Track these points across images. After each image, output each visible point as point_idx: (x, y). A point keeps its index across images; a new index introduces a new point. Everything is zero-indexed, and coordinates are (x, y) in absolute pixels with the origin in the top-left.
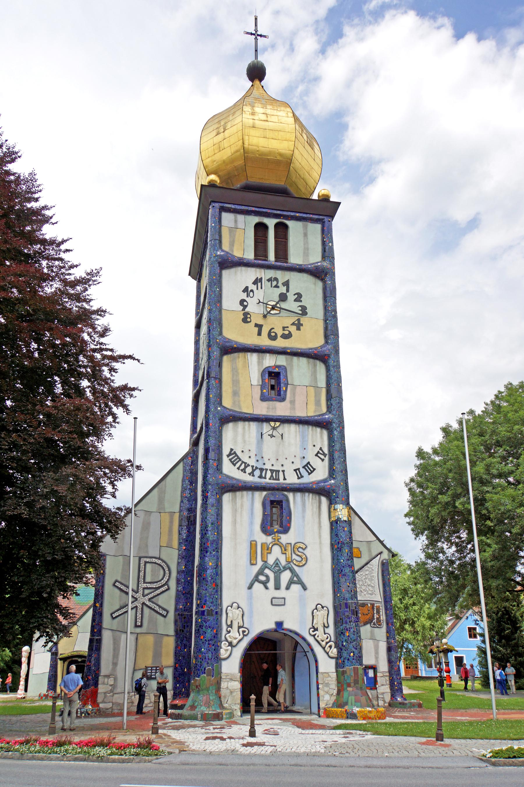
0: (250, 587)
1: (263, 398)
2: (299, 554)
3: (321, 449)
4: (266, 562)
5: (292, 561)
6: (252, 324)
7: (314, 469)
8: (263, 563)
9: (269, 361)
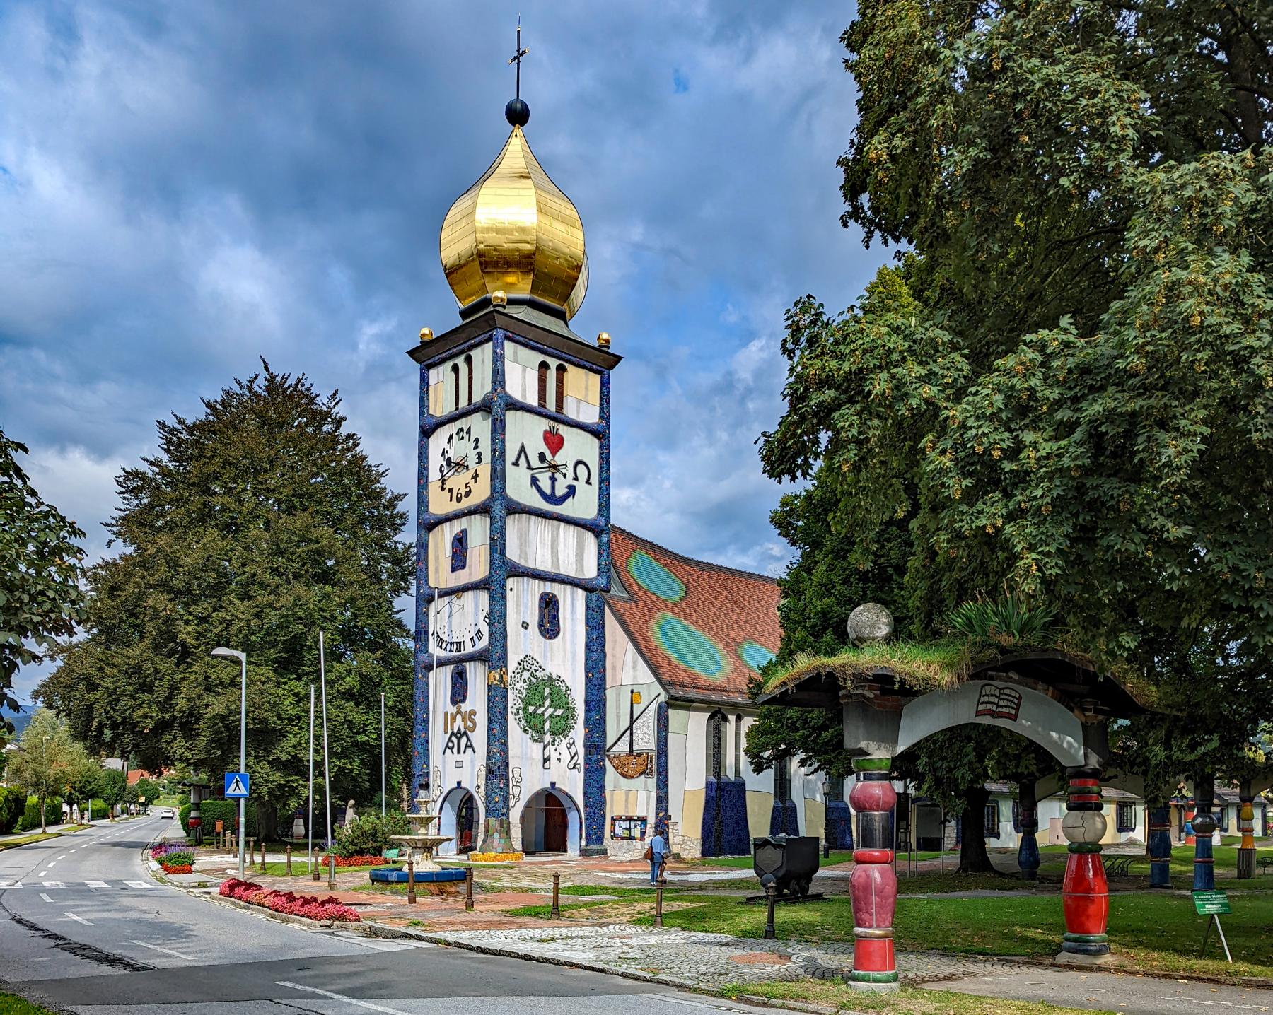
6: (447, 490)
9: (457, 526)
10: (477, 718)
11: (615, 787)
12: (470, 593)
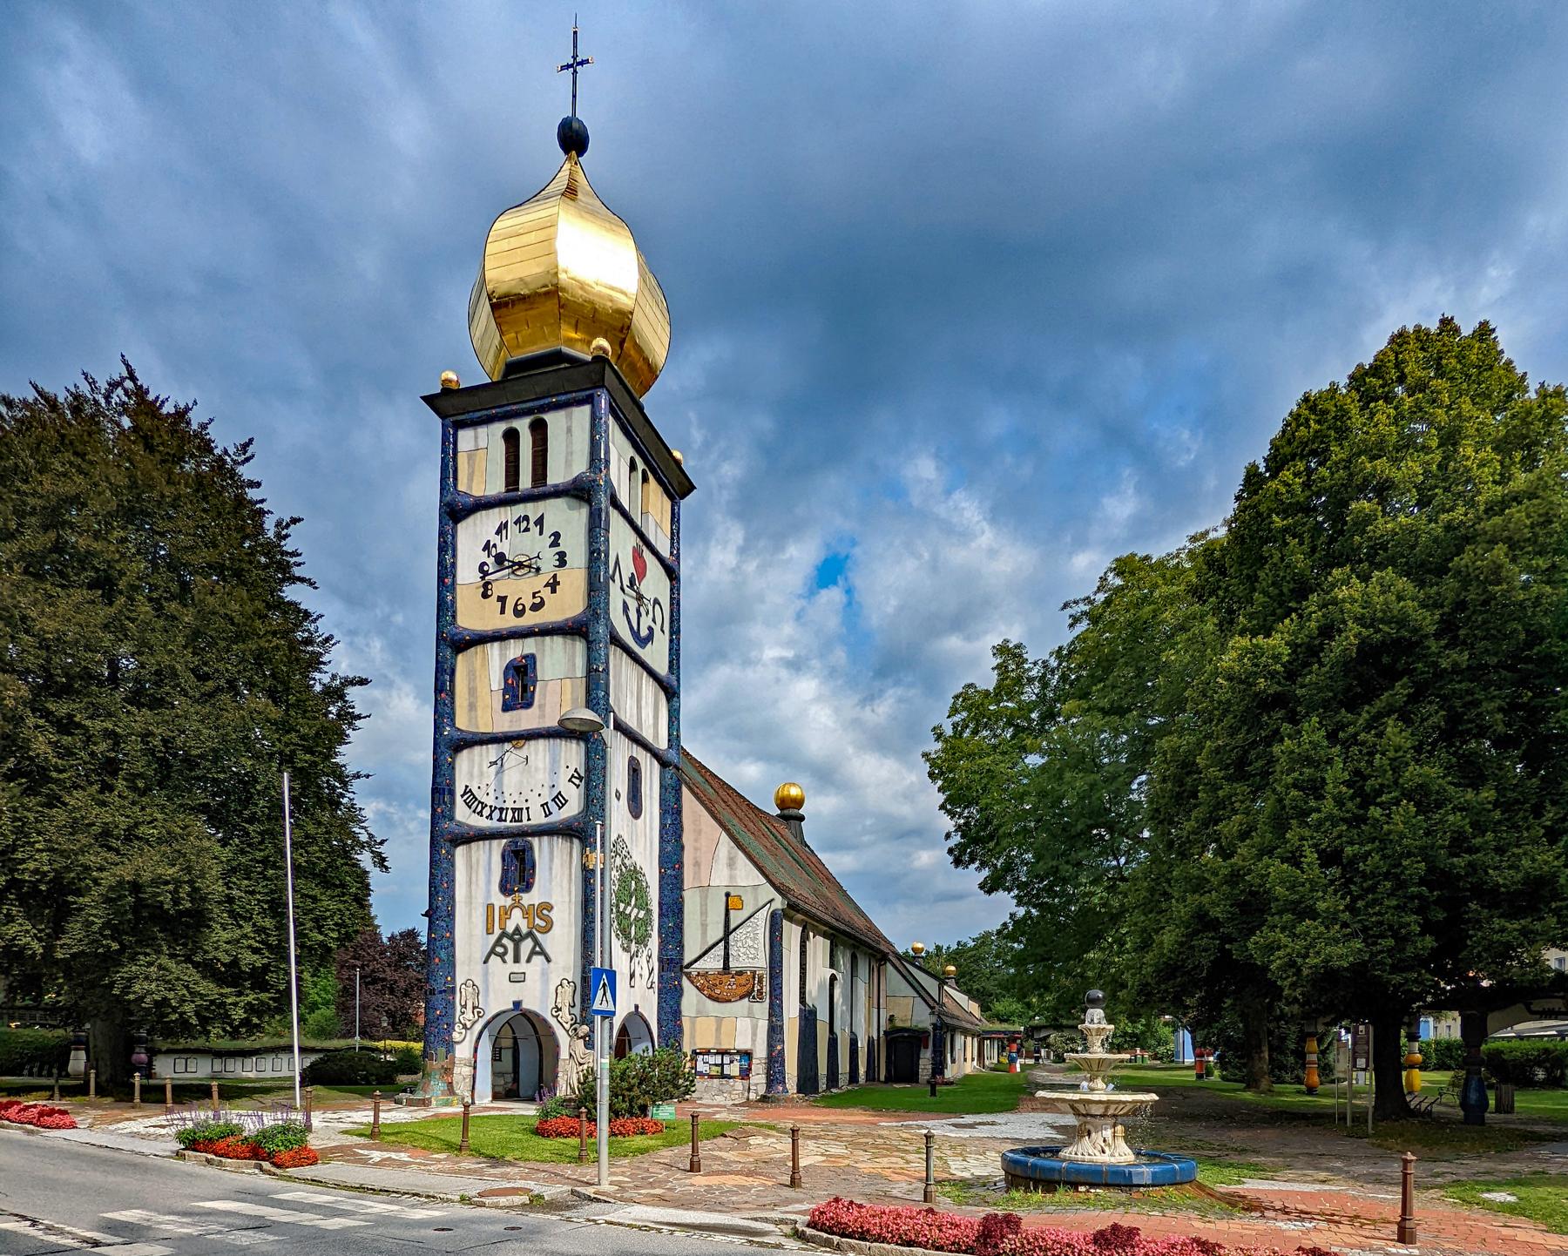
1: (506, 707)
6: (494, 598)
9: (515, 650)
10: (554, 915)
11: (698, 1012)
12: (541, 743)
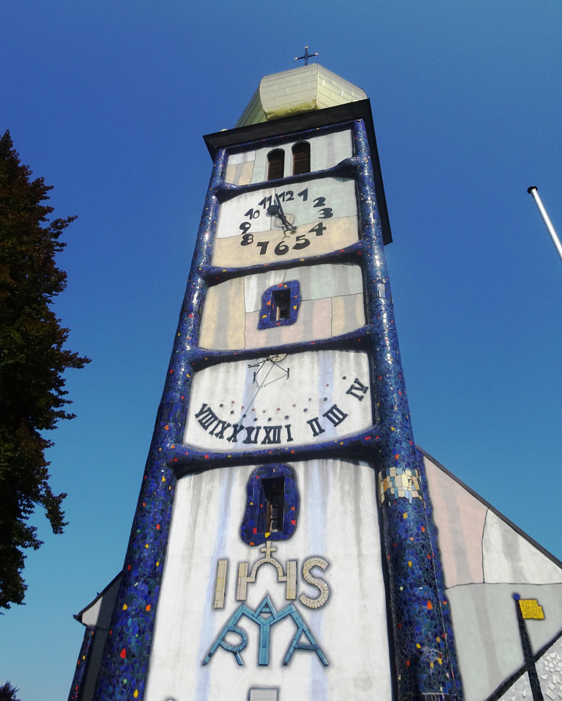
0: (205, 664)
1: (263, 325)
2: (312, 580)
3: (357, 381)
4: (243, 602)
5: (297, 598)
7: (345, 416)
8: (239, 604)
10: (332, 576)
12: (307, 357)
